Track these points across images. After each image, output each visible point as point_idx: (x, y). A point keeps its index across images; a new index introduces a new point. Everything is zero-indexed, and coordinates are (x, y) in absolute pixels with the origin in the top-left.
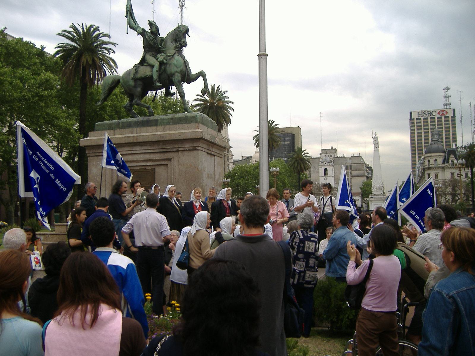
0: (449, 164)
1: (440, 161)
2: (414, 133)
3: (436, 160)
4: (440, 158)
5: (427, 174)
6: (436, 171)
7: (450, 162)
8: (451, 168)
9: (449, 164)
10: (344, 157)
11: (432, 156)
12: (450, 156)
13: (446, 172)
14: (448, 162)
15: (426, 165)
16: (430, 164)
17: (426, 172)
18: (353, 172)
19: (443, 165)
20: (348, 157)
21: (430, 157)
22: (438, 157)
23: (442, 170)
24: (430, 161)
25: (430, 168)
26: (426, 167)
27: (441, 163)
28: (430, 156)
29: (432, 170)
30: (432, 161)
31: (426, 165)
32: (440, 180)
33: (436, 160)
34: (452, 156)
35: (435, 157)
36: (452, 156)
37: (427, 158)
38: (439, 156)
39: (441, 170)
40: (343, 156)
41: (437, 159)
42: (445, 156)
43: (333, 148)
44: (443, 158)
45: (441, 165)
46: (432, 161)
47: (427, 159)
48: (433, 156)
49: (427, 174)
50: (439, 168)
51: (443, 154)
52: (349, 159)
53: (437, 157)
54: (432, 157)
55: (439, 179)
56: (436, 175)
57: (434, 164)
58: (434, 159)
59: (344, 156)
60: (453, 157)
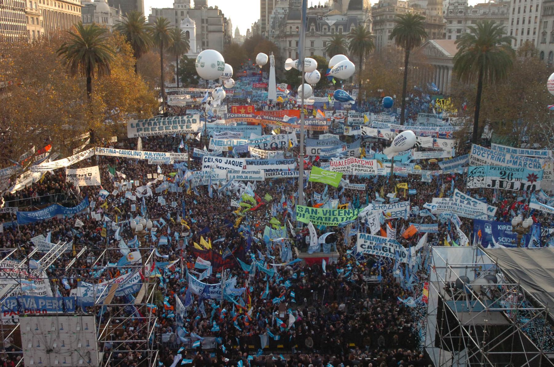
7: (311, 30)
18: (209, 27)
25: (291, 36)
30: (294, 28)
34: (313, 24)
36: (313, 24)
46: (294, 28)
58: (296, 26)
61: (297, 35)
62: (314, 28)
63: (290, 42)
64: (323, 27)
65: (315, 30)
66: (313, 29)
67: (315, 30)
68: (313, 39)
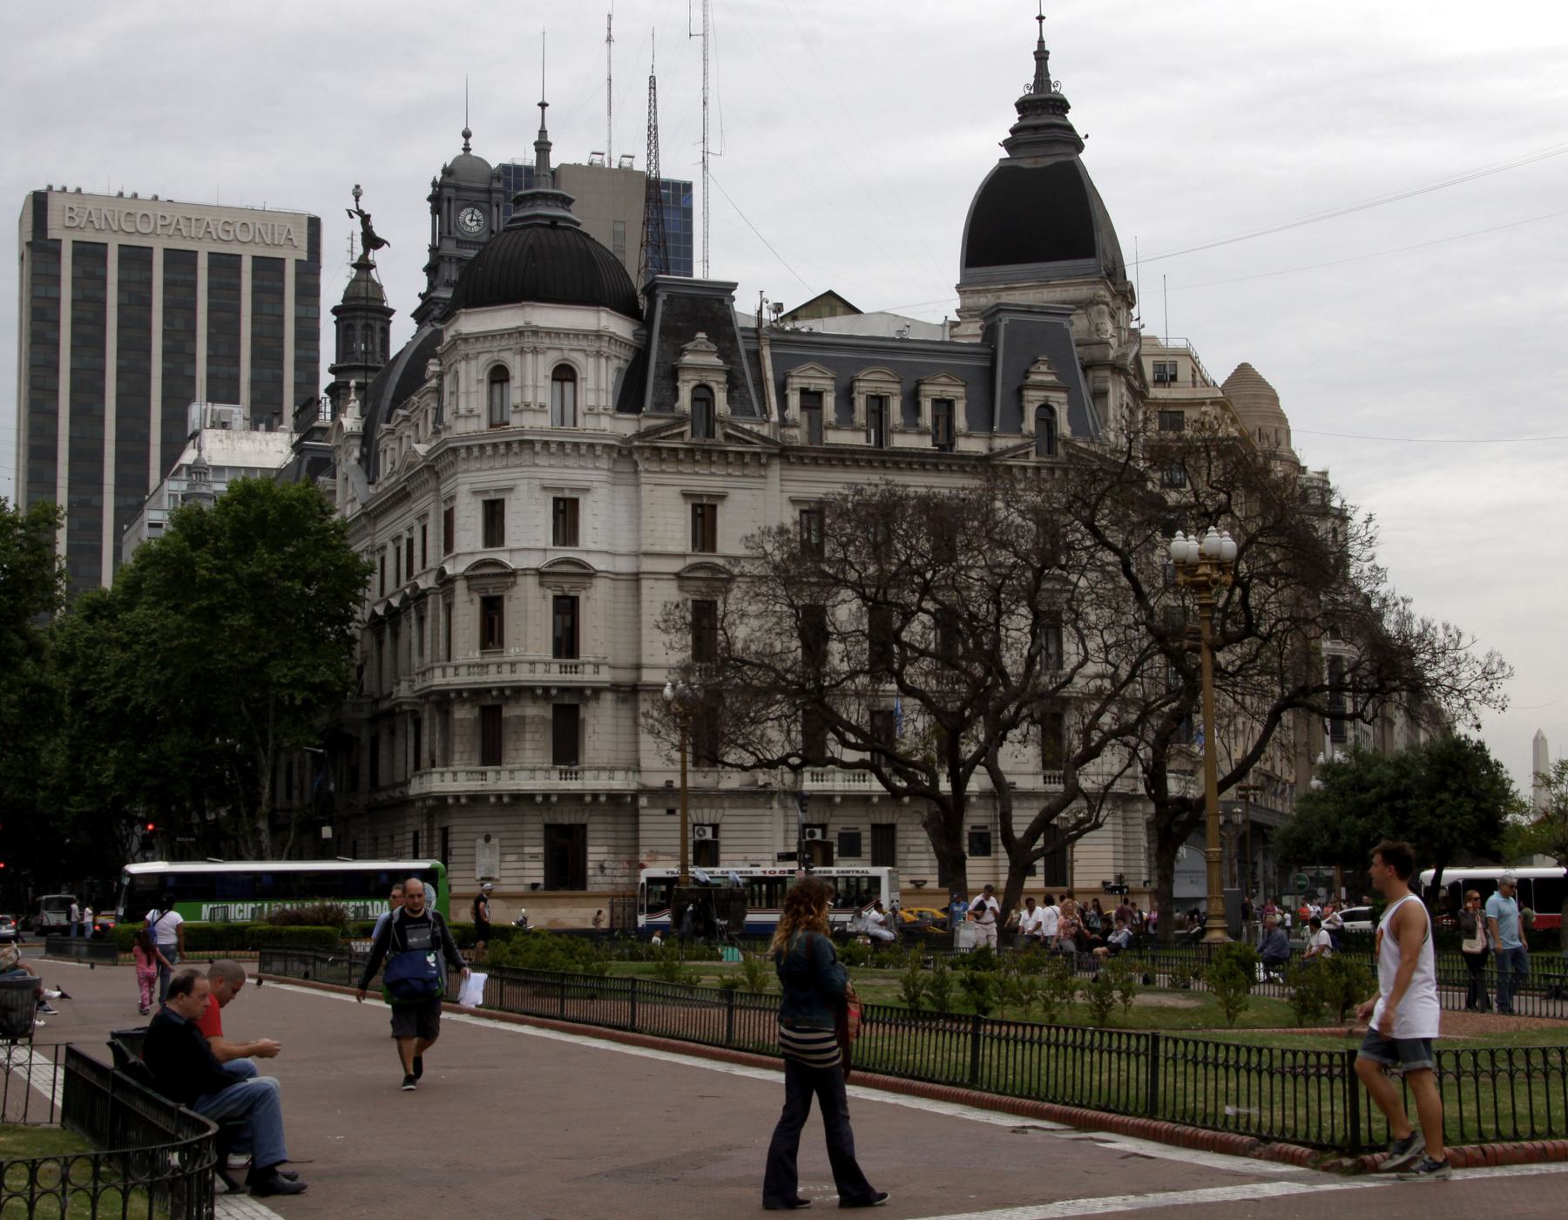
3: (564, 374)
4: (598, 354)
6: (569, 474)
7: (685, 401)
8: (690, 452)
9: (681, 420)
11: (536, 332)
13: (645, 489)
16: (515, 397)
19: (627, 426)
22: (584, 344)
24: (515, 372)
27: (607, 400)
28: (520, 332)
32: (597, 563)
33: (564, 374)
35: (556, 342)
37: (479, 346)
38: (598, 335)
44: (622, 364)
45: (606, 423)
47: (484, 358)
50: (586, 449)
51: (617, 325)
53: (575, 344)
54: (530, 341)
55: (588, 552)
56: (566, 515)
64: (796, 383)
66: (703, 395)
68: (707, 481)
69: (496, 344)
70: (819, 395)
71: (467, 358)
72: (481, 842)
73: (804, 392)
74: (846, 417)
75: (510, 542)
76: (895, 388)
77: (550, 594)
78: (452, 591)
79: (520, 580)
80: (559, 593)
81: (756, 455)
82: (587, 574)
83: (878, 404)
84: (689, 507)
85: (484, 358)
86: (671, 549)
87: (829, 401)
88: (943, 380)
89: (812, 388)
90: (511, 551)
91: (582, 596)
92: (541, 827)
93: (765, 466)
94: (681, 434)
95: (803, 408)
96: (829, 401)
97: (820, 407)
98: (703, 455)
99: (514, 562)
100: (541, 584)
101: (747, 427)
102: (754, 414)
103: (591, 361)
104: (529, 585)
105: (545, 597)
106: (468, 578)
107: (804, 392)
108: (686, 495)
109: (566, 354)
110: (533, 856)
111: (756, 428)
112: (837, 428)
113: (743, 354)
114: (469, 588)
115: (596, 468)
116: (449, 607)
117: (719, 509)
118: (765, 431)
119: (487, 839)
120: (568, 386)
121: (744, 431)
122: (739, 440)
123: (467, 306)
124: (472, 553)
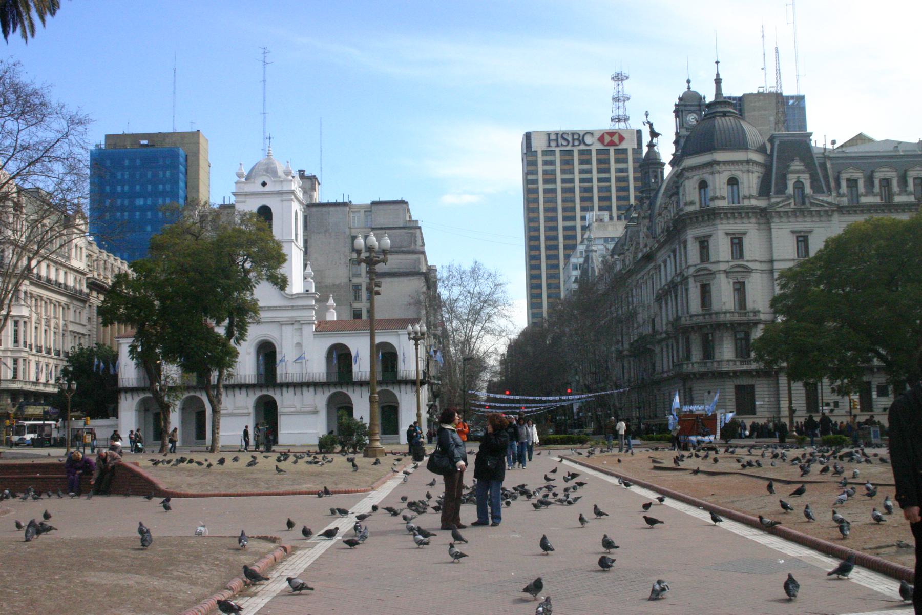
0: (789, 198)
1: (750, 182)
2: (536, 191)
3: (733, 181)
4: (748, 171)
5: (696, 238)
6: (735, 226)
7: (790, 190)
8: (794, 212)
9: (789, 198)
10: (344, 204)
11: (718, 163)
12: (788, 166)
14: (781, 190)
15: (692, 203)
16: (710, 194)
17: (691, 234)
19: (762, 203)
20: (360, 206)
21: (709, 170)
22: (741, 167)
23: (759, 224)
24: (710, 183)
25: (709, 214)
26: (691, 208)
27: (754, 192)
28: (711, 164)
29: (718, 222)
30: (719, 184)
31: (692, 203)
32: (751, 265)
33: (733, 181)
34: (797, 165)
35: (728, 167)
36: (797, 165)
37: (693, 173)
38: (748, 162)
39: (753, 220)
40: (340, 200)
41: (738, 174)
42: (768, 167)
43: (306, 174)
44: (761, 175)
45: (754, 202)
47: (696, 178)
48: (725, 163)
49: (696, 238)
52: (362, 211)
54: (717, 168)
55: (748, 261)
56: (737, 243)
57: (724, 198)
59: (346, 200)
60: (802, 167)
61: (737, 212)
62: (806, 179)
63: (704, 243)
64: (844, 176)
65: (808, 190)
66: (799, 185)
67: (808, 190)
68: (802, 225)
69: (701, 172)
70: (856, 181)
71: (688, 178)
72: (706, 394)
73: (848, 180)
74: (870, 191)
75: (712, 259)
76: (894, 174)
77: (731, 281)
78: (688, 283)
79: (717, 276)
80: (736, 281)
81: (826, 211)
82: (749, 271)
83: (886, 183)
84: (795, 238)
85: (696, 178)
86: (787, 257)
87: (861, 184)
88: (918, 168)
89: (852, 178)
90: (714, 263)
91: (746, 281)
92: (733, 387)
93: (831, 216)
94: (789, 204)
95: (848, 186)
96: (861, 184)
97: (857, 186)
98: (801, 212)
99: (713, 268)
100: (727, 277)
101: (821, 198)
102: (823, 192)
103: (745, 175)
104: (722, 277)
105: (729, 283)
106: (694, 276)
107: (848, 180)
108: (793, 232)
109: (734, 173)
110: (730, 400)
111: (825, 199)
112: (866, 195)
113: (817, 164)
114: (695, 281)
115: (750, 223)
116: (687, 290)
117: (810, 238)
118: (829, 199)
119: (709, 392)
120: (735, 187)
121: (818, 200)
122: (817, 205)
123: (687, 156)
124: (695, 266)
